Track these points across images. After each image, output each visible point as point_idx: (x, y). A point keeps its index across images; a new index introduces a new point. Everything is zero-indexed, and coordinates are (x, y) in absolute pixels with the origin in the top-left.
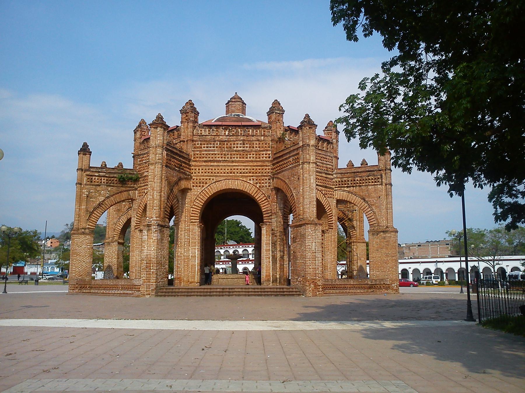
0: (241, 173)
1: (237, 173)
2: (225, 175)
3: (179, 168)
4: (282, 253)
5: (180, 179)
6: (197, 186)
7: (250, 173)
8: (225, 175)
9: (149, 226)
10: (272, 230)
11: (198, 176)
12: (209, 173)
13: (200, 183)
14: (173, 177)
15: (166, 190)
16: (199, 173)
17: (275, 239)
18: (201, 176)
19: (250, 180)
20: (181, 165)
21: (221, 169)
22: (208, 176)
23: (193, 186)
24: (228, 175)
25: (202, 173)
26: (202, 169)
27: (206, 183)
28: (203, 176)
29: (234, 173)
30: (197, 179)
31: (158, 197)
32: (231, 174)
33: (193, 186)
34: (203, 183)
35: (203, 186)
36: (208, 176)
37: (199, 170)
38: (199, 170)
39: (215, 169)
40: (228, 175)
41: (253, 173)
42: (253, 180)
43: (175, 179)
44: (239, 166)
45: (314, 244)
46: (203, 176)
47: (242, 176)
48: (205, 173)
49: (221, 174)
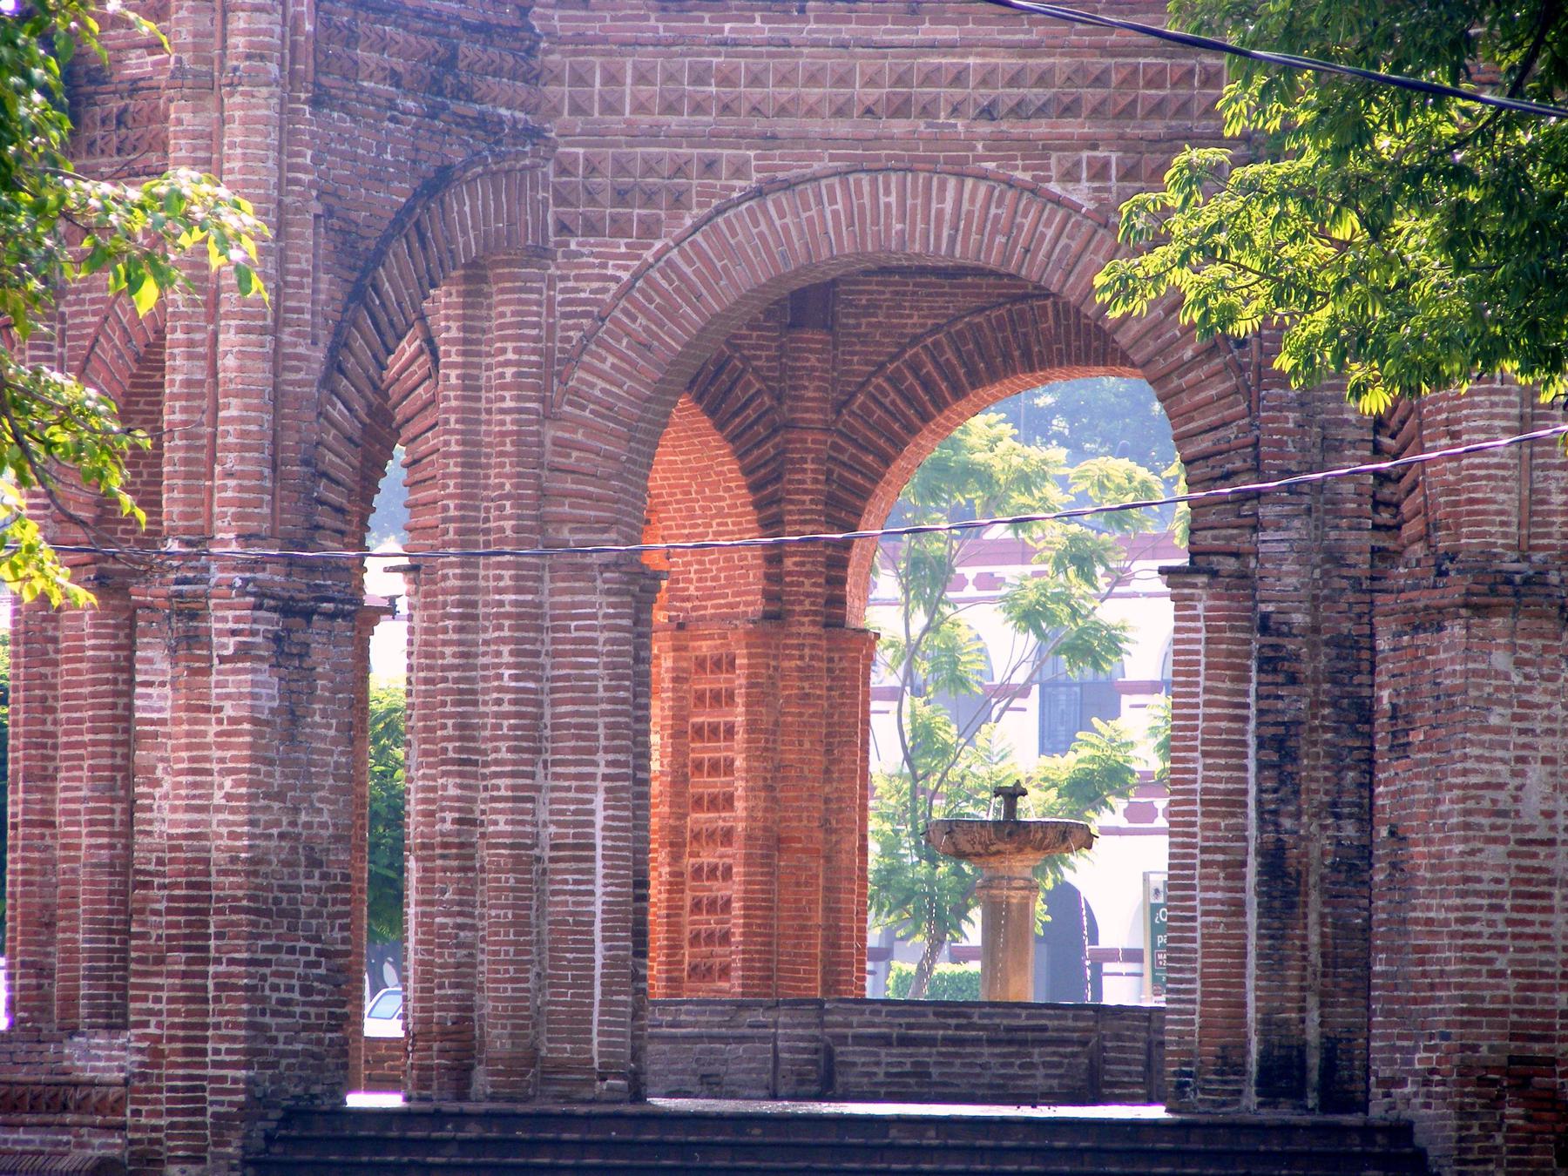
0: (988, 113)
1: (955, 111)
2: (841, 128)
3: (435, 86)
4: (1350, 830)
5: (437, 184)
6: (592, 228)
7: (1069, 109)
8: (841, 128)
9: (189, 614)
10: (1265, 625)
11: (598, 136)
12: (698, 108)
13: (621, 196)
14: (378, 177)
15: (320, 292)
16: (610, 108)
17: (1294, 704)
18: (635, 136)
19: (1070, 176)
20: (449, 63)
21: (813, 79)
22: (689, 137)
23: (563, 228)
24: (869, 128)
25: (640, 108)
26: (642, 78)
27: (678, 201)
28: (652, 136)
29: (927, 111)
30: (592, 169)
31: (261, 372)
32: (899, 127)
33: (563, 228)
34: (650, 198)
35: (650, 230)
36: (689, 137)
37: (612, 78)
38: (612, 78)
39: (755, 80)
40: (869, 128)
41: (1097, 112)
42: (1100, 172)
43: (399, 194)
44: (966, 46)
45: (1536, 773)
46: (652, 136)
47: (997, 143)
48: (671, 108)
49: (815, 127)
